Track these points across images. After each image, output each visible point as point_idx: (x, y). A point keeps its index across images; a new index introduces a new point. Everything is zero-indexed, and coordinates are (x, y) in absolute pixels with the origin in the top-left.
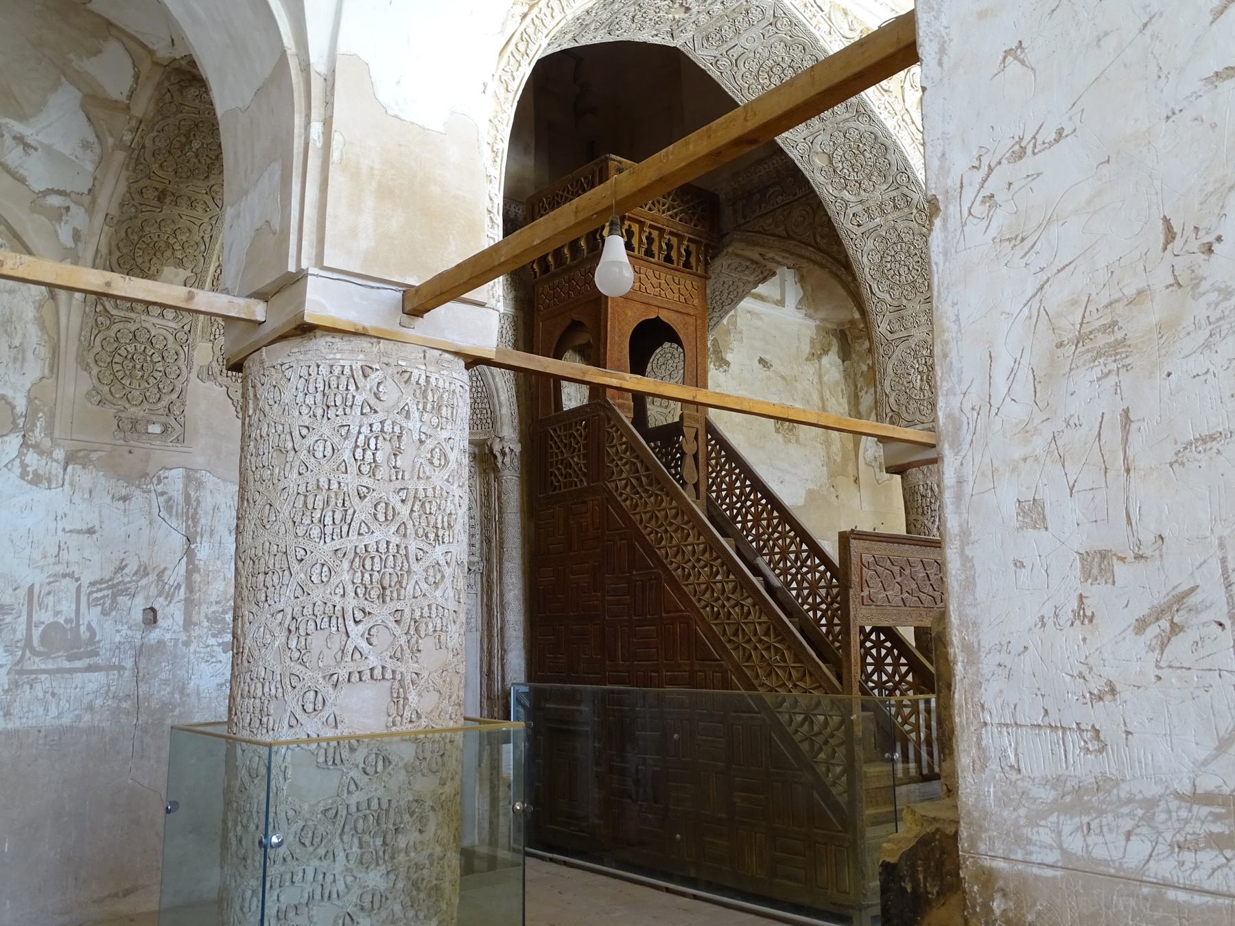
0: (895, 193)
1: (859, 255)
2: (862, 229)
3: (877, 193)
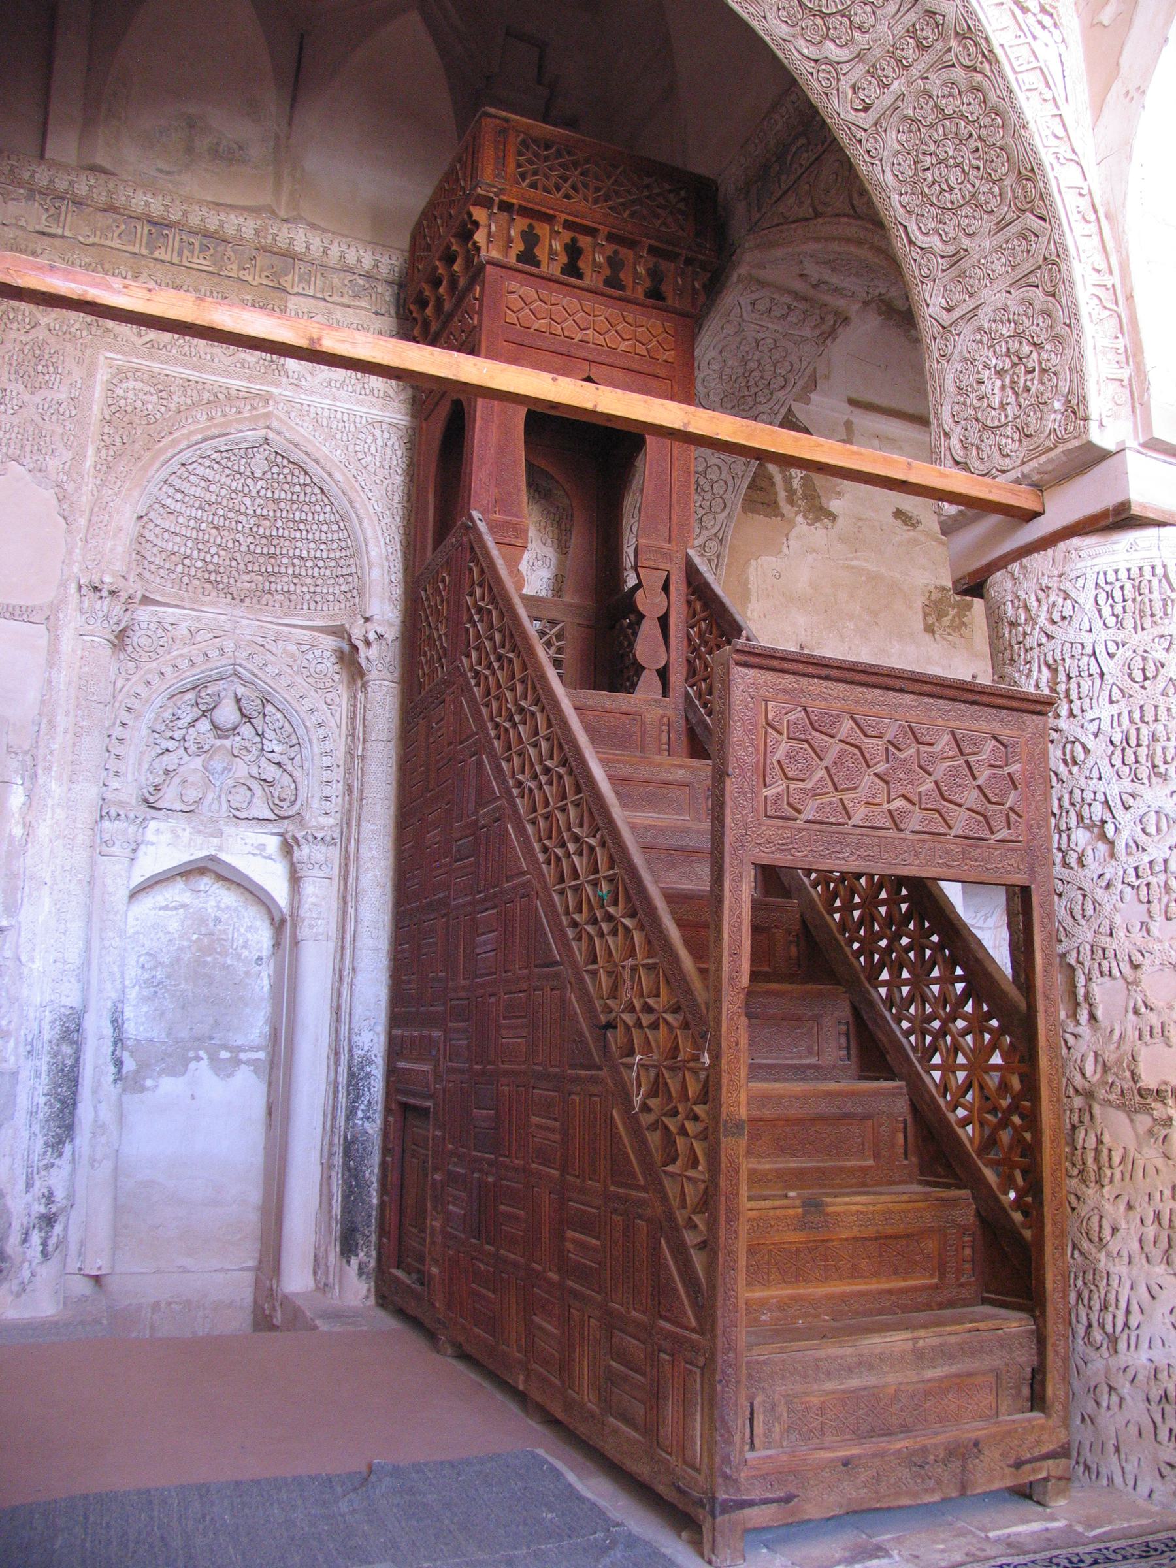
0: (912, 17)
1: (878, 169)
2: (873, 114)
3: (883, 27)
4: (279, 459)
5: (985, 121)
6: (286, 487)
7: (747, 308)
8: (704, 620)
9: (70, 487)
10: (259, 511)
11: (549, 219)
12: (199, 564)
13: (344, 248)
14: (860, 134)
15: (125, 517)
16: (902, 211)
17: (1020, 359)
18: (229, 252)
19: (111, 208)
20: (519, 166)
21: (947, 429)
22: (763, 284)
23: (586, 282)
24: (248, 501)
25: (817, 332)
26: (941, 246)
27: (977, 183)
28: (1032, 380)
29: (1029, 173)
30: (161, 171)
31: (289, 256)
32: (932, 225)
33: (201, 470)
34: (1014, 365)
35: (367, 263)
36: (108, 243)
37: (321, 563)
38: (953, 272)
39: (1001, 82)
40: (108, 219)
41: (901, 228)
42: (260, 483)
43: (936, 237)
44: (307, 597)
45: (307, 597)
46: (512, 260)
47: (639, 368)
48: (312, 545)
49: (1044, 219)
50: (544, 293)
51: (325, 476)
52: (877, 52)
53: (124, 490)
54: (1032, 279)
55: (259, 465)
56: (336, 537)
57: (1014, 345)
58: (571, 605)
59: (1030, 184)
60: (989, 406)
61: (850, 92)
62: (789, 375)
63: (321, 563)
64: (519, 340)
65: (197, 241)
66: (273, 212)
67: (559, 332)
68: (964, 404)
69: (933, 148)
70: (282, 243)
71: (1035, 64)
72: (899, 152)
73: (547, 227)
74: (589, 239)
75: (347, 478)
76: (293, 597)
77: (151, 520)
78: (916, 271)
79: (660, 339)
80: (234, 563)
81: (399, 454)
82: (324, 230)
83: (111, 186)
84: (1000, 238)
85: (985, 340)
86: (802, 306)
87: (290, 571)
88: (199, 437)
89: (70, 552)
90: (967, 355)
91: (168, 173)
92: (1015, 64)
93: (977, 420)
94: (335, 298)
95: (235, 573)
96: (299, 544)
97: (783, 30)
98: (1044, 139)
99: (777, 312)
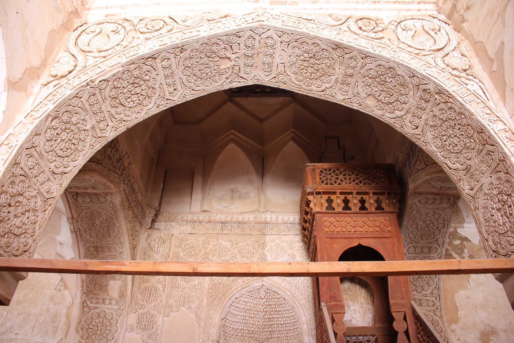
0: (419, 93)
2: (420, 129)
4: (269, 291)
5: (457, 118)
6: (273, 300)
7: (418, 204)
8: (422, 330)
9: (199, 312)
10: (265, 310)
11: (335, 193)
12: (246, 332)
13: (283, 216)
14: (418, 137)
15: (217, 319)
16: (443, 158)
17: (504, 202)
18: (247, 226)
19: (210, 222)
20: (321, 179)
21: (486, 238)
22: (420, 194)
23: (353, 210)
24: (261, 307)
25: (449, 205)
26: (461, 166)
27: (465, 140)
28: (511, 210)
29: (481, 130)
30: (224, 207)
31: (266, 223)
32: (455, 160)
33: (243, 299)
34: (503, 205)
35: (291, 219)
36: (209, 232)
37: (288, 325)
38: (468, 175)
39: (458, 103)
40: (209, 225)
41: (445, 164)
42: (264, 300)
43: (458, 164)
44: (285, 338)
45: (285, 338)
46: (324, 210)
47: (378, 236)
48: (284, 319)
49: (493, 145)
50: (337, 219)
51: (284, 294)
52: (412, 108)
53: (216, 311)
54: (498, 169)
55: (262, 294)
56: (291, 315)
57: (500, 197)
58: (378, 328)
59: (483, 134)
60: (499, 225)
61: (409, 124)
62: (444, 222)
63: (288, 325)
64: (331, 236)
65: (236, 225)
66: (259, 211)
67: (345, 230)
68: (489, 226)
69: (444, 133)
70: (263, 220)
71: (469, 93)
72: (434, 138)
73: (335, 196)
74: (351, 196)
75: (292, 294)
76: (280, 339)
77: (227, 319)
78: (456, 178)
79: (384, 223)
80: (258, 329)
81: (310, 281)
82: (276, 212)
83: (209, 215)
84: (480, 157)
85: (489, 198)
86: (439, 197)
87: (278, 329)
88: (240, 289)
89: (200, 335)
90: (484, 206)
91: (226, 207)
92: (461, 96)
93: (496, 232)
94: (282, 233)
95: (259, 333)
96: (280, 319)
97: (380, 112)
98: (482, 116)
99: (430, 202)
